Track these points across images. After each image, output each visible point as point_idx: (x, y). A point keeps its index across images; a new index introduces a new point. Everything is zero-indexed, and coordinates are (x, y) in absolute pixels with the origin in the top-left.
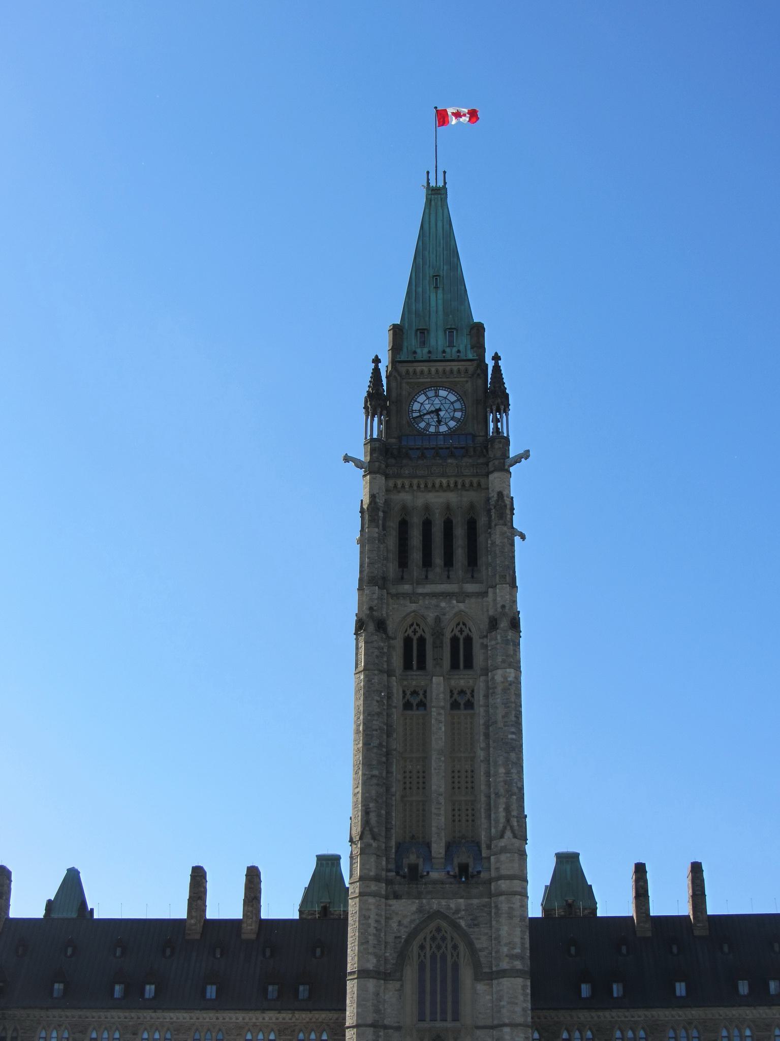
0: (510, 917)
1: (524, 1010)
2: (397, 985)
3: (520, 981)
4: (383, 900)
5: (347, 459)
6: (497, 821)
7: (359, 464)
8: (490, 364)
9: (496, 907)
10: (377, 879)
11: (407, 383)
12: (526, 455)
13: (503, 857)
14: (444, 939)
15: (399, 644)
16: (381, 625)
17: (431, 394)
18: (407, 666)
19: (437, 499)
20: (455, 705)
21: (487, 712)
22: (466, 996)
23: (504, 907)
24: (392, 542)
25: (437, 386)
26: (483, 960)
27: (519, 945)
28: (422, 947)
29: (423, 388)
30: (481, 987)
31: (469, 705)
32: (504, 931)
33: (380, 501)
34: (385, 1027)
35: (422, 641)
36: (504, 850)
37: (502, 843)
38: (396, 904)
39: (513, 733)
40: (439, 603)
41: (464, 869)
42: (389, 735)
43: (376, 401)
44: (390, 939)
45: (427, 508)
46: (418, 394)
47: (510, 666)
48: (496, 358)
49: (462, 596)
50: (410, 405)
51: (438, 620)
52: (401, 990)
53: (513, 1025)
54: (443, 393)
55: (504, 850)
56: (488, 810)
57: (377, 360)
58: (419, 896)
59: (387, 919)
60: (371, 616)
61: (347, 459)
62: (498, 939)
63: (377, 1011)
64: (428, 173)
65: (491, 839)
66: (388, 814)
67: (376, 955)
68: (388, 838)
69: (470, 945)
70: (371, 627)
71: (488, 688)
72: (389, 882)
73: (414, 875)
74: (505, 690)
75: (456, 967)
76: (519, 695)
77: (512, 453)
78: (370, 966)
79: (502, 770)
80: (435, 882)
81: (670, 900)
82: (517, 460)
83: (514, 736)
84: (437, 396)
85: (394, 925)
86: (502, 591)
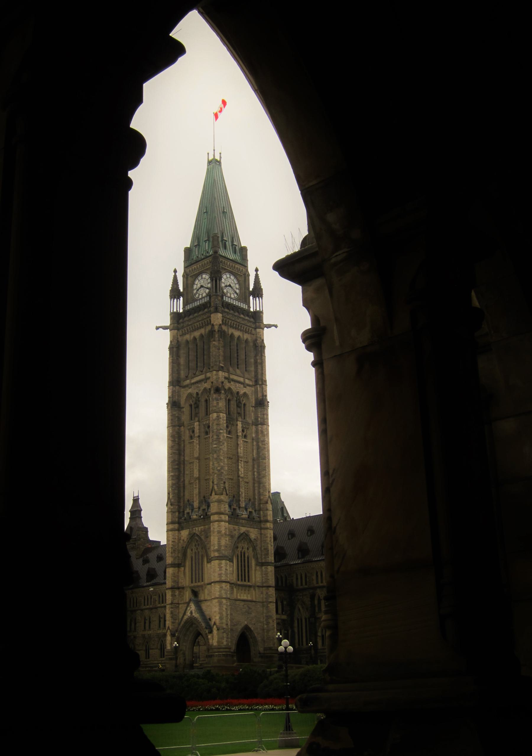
4: (177, 532)
5: (157, 328)
7: (165, 328)
11: (191, 276)
17: (200, 278)
19: (197, 334)
27: (216, 545)
28: (192, 550)
30: (209, 565)
39: (215, 444)
45: (195, 339)
46: (195, 280)
50: (192, 287)
54: (204, 276)
57: (175, 271)
61: (157, 328)
63: (174, 581)
64: (208, 154)
83: (216, 446)
84: (202, 278)
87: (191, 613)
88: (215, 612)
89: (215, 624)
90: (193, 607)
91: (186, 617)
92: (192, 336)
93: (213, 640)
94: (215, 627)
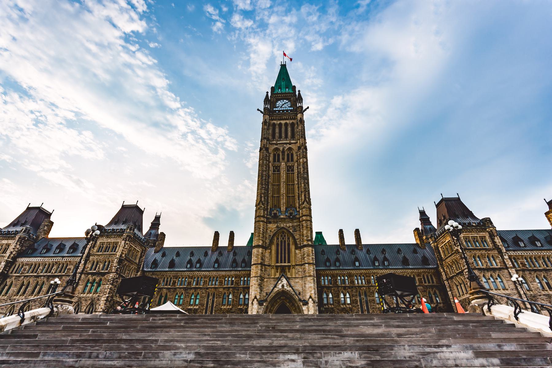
0: (307, 228)
1: (313, 258)
2: (269, 251)
3: (310, 248)
5: (258, 110)
6: (301, 199)
7: (261, 112)
8: (297, 93)
9: (302, 225)
10: (263, 217)
12: (308, 108)
13: (304, 210)
14: (285, 236)
15: (272, 155)
16: (267, 149)
18: (274, 161)
20: (288, 170)
21: (298, 171)
22: (292, 254)
23: (305, 225)
24: (270, 131)
25: (283, 99)
26: (298, 242)
28: (278, 239)
29: (280, 100)
30: (297, 251)
31: (293, 170)
32: (305, 232)
33: (268, 121)
34: (265, 265)
35: (279, 155)
36: (304, 207)
37: (303, 206)
38: (270, 225)
40: (284, 144)
41: (291, 214)
42: (269, 178)
43: (266, 100)
44: (267, 236)
45: (281, 124)
47: (304, 158)
48: (299, 91)
49: (290, 144)
51: (283, 149)
52: (271, 252)
53: (309, 264)
55: (304, 207)
56: (299, 197)
57: (267, 92)
58: (277, 223)
59: (266, 230)
60: (264, 147)
61: (258, 110)
62: (303, 235)
63: (262, 259)
65: (300, 205)
66: (268, 199)
67: (262, 241)
68: (267, 206)
69: (294, 237)
70: (264, 149)
71: (298, 164)
72: (267, 218)
73: (275, 216)
74: (303, 164)
75: (289, 245)
76: (307, 166)
77: (304, 109)
78: (260, 244)
79: (303, 185)
80: (282, 218)
81: (350, 240)
82: (306, 110)
85: (269, 232)
86: (301, 141)
87: (283, 286)
88: (311, 287)
89: (311, 297)
90: (285, 281)
91: (276, 289)
92: (279, 122)
93: (308, 311)
94: (311, 300)
